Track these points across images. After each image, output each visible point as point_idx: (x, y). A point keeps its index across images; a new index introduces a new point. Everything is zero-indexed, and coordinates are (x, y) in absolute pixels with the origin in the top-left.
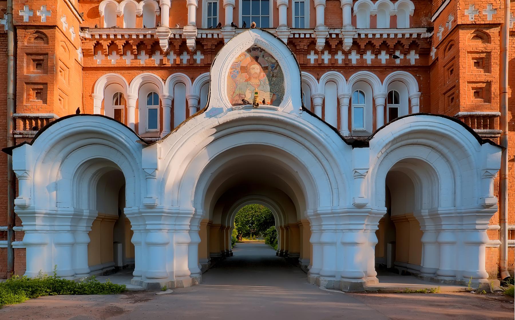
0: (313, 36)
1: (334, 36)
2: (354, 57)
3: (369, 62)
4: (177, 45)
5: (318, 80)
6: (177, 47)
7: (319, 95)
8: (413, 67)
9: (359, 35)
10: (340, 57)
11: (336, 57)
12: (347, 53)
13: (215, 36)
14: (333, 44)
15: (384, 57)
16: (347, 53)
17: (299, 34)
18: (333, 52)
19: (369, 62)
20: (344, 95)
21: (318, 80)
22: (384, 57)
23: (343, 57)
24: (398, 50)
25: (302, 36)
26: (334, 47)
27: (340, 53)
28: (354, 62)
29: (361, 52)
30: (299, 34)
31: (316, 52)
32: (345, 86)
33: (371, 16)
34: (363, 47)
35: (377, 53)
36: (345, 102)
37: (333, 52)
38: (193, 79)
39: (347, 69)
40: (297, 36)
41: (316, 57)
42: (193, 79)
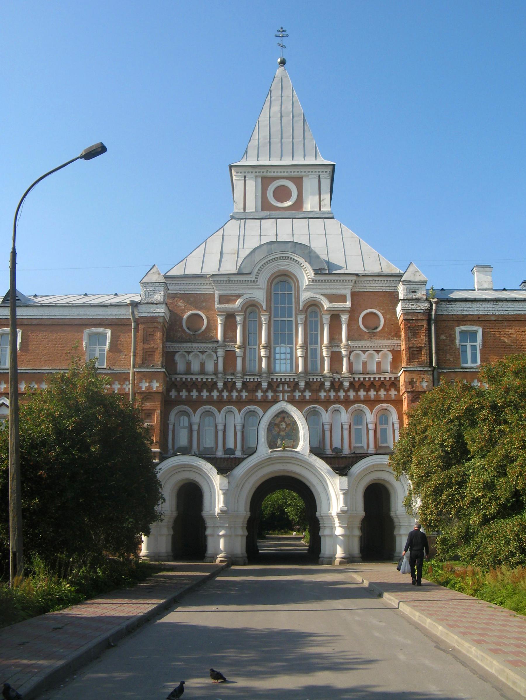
0: (322, 380)
1: (337, 380)
2: (352, 394)
3: (362, 397)
4: (229, 385)
5: (327, 411)
6: (229, 388)
7: (328, 422)
8: (394, 400)
9: (354, 378)
10: (342, 394)
11: (339, 394)
12: (346, 391)
13: (256, 380)
14: (337, 385)
15: (372, 393)
16: (346, 391)
17: (313, 379)
18: (337, 391)
19: (362, 397)
20: (345, 422)
21: (327, 411)
22: (372, 393)
23: (344, 394)
24: (382, 388)
25: (315, 380)
26: (337, 387)
27: (342, 391)
28: (352, 397)
29: (357, 391)
30: (313, 379)
31: (325, 391)
32: (345, 416)
33: (363, 363)
34: (357, 387)
35: (368, 391)
36: (346, 427)
37: (337, 391)
38: (240, 411)
39: (347, 403)
40: (311, 380)
41: (325, 394)
42: (240, 411)
